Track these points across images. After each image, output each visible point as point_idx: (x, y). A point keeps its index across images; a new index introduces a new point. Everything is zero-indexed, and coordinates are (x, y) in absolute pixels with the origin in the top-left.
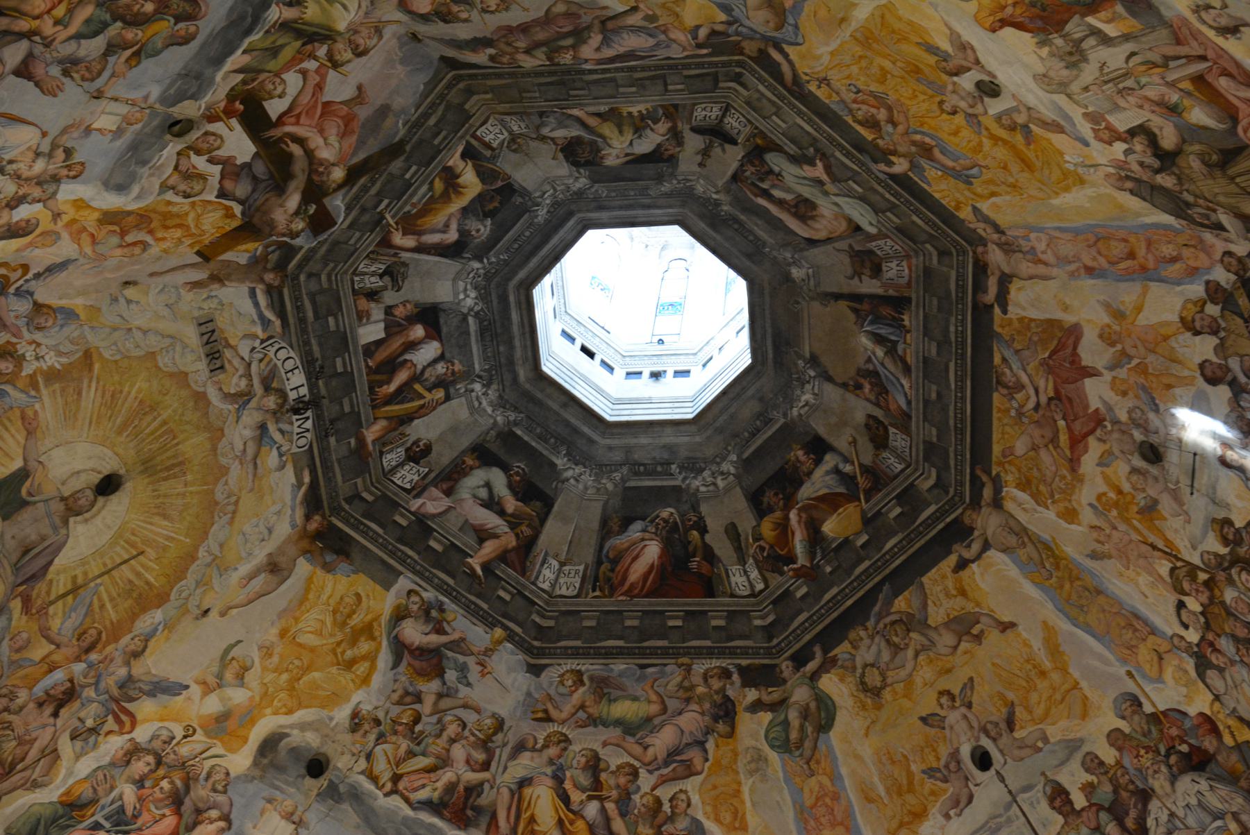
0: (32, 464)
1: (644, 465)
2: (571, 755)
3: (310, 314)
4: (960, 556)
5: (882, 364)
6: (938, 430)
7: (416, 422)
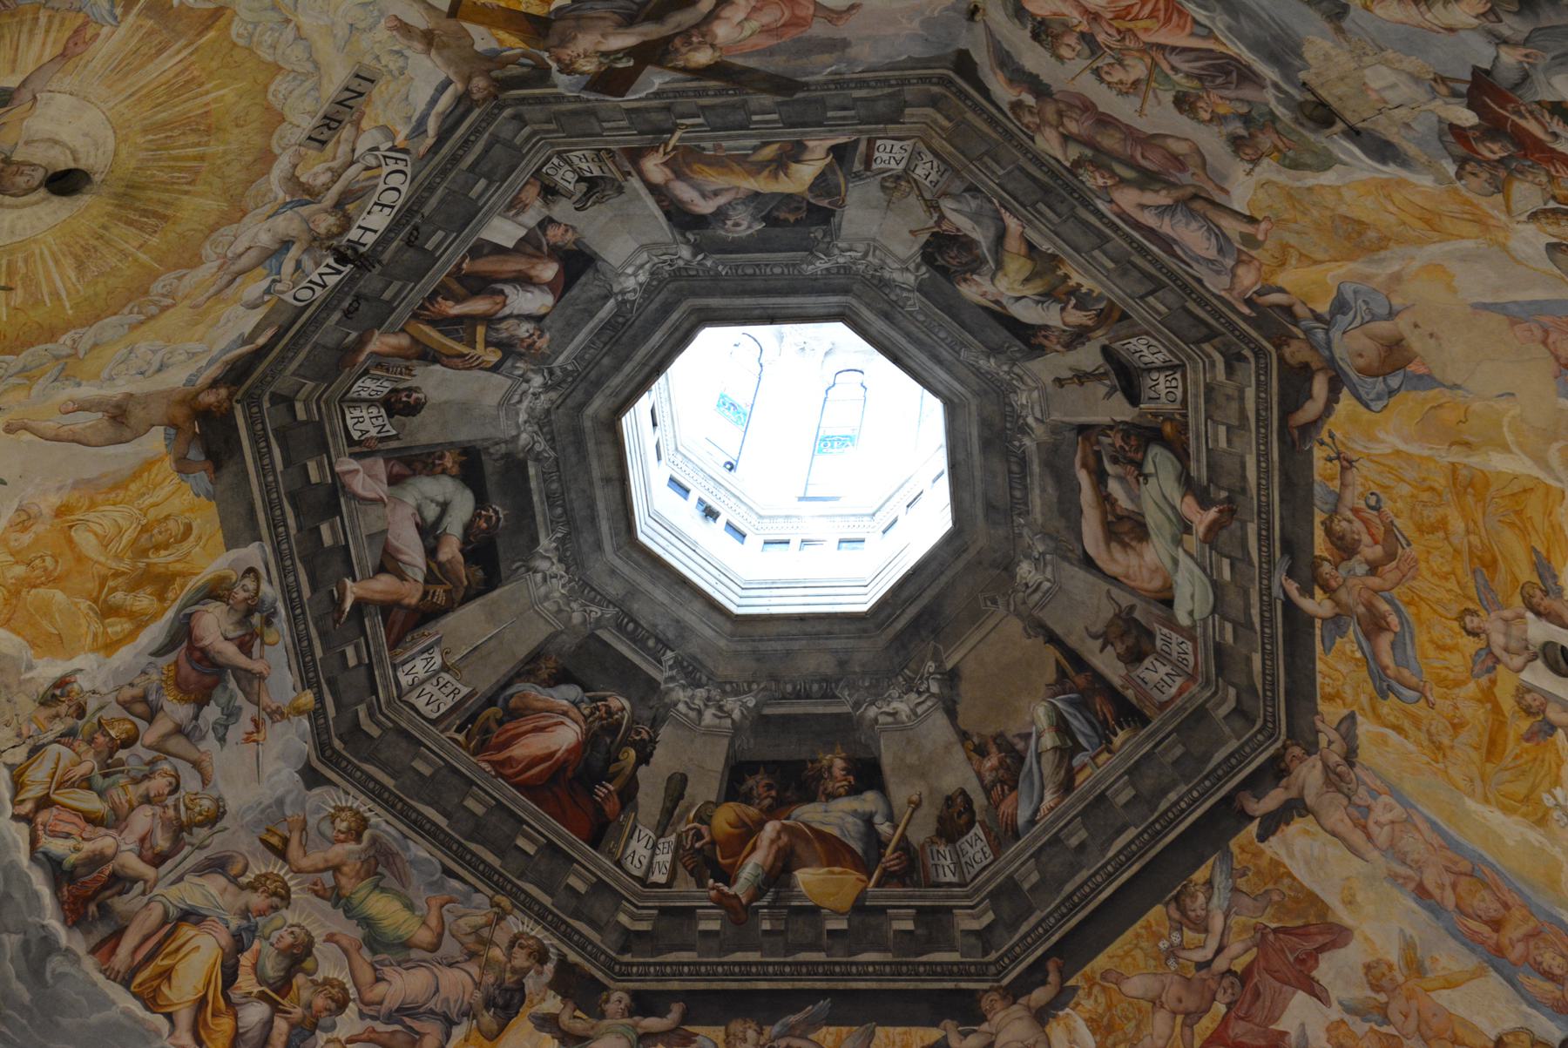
0: (26, 95)
1: (637, 624)
2: (278, 923)
3: (470, 159)
4: (945, 1037)
5: (1039, 756)
6: (1042, 880)
7: (437, 367)
